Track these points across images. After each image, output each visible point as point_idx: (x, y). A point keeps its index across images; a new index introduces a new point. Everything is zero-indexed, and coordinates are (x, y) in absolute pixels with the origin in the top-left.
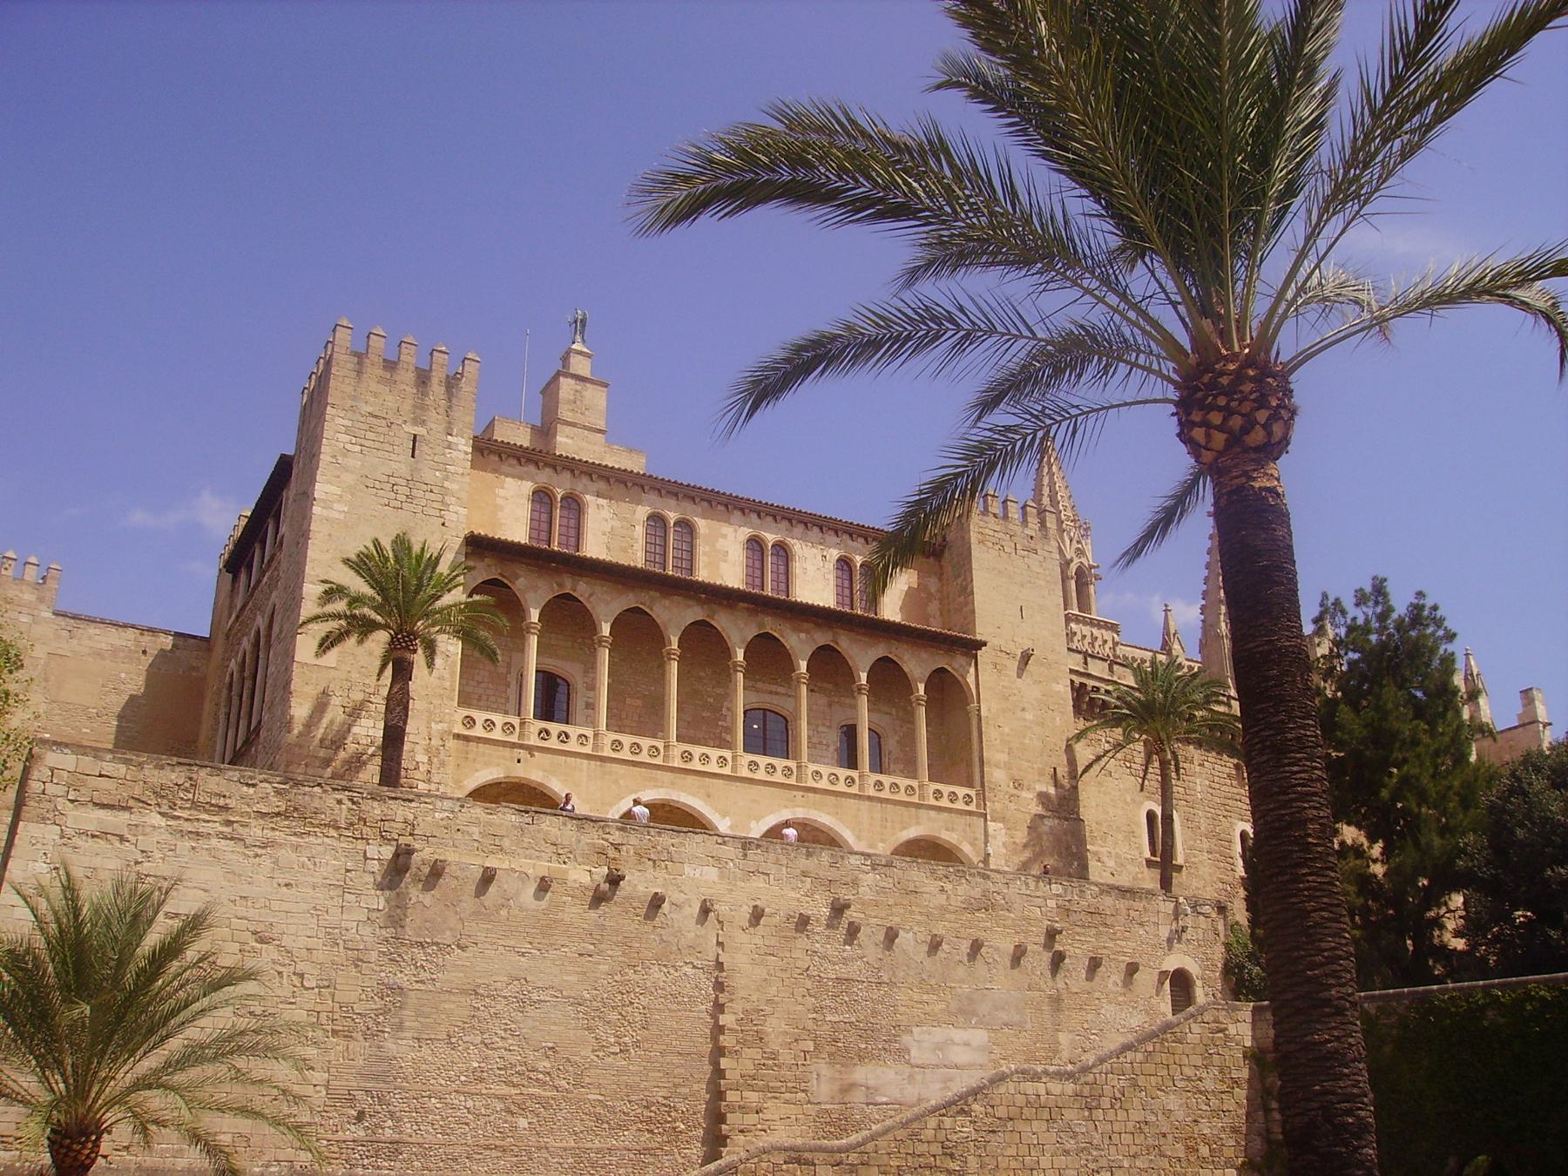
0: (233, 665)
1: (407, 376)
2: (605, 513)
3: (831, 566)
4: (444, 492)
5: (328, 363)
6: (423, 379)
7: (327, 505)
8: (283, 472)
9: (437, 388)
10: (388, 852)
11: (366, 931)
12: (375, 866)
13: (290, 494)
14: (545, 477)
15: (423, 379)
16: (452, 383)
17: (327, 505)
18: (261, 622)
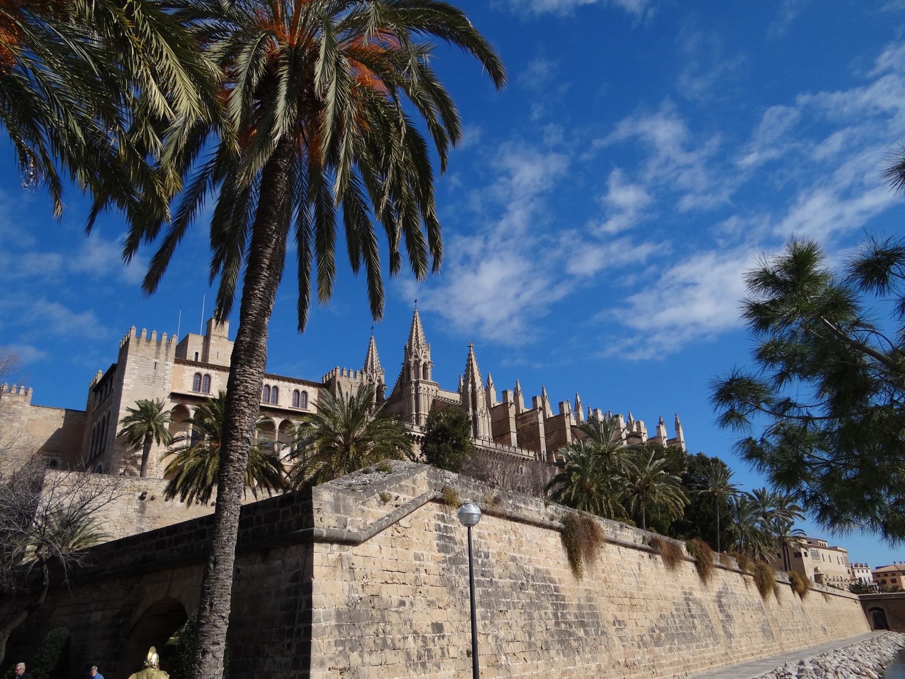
0: (95, 424)
1: (153, 343)
2: (218, 380)
3: (291, 393)
4: (165, 379)
5: (128, 339)
6: (159, 343)
7: (128, 385)
8: (113, 368)
9: (163, 347)
10: (140, 494)
11: (134, 514)
12: (137, 498)
13: (116, 376)
14: (198, 370)
15: (159, 343)
16: (168, 345)
17: (128, 385)
18: (105, 414)
